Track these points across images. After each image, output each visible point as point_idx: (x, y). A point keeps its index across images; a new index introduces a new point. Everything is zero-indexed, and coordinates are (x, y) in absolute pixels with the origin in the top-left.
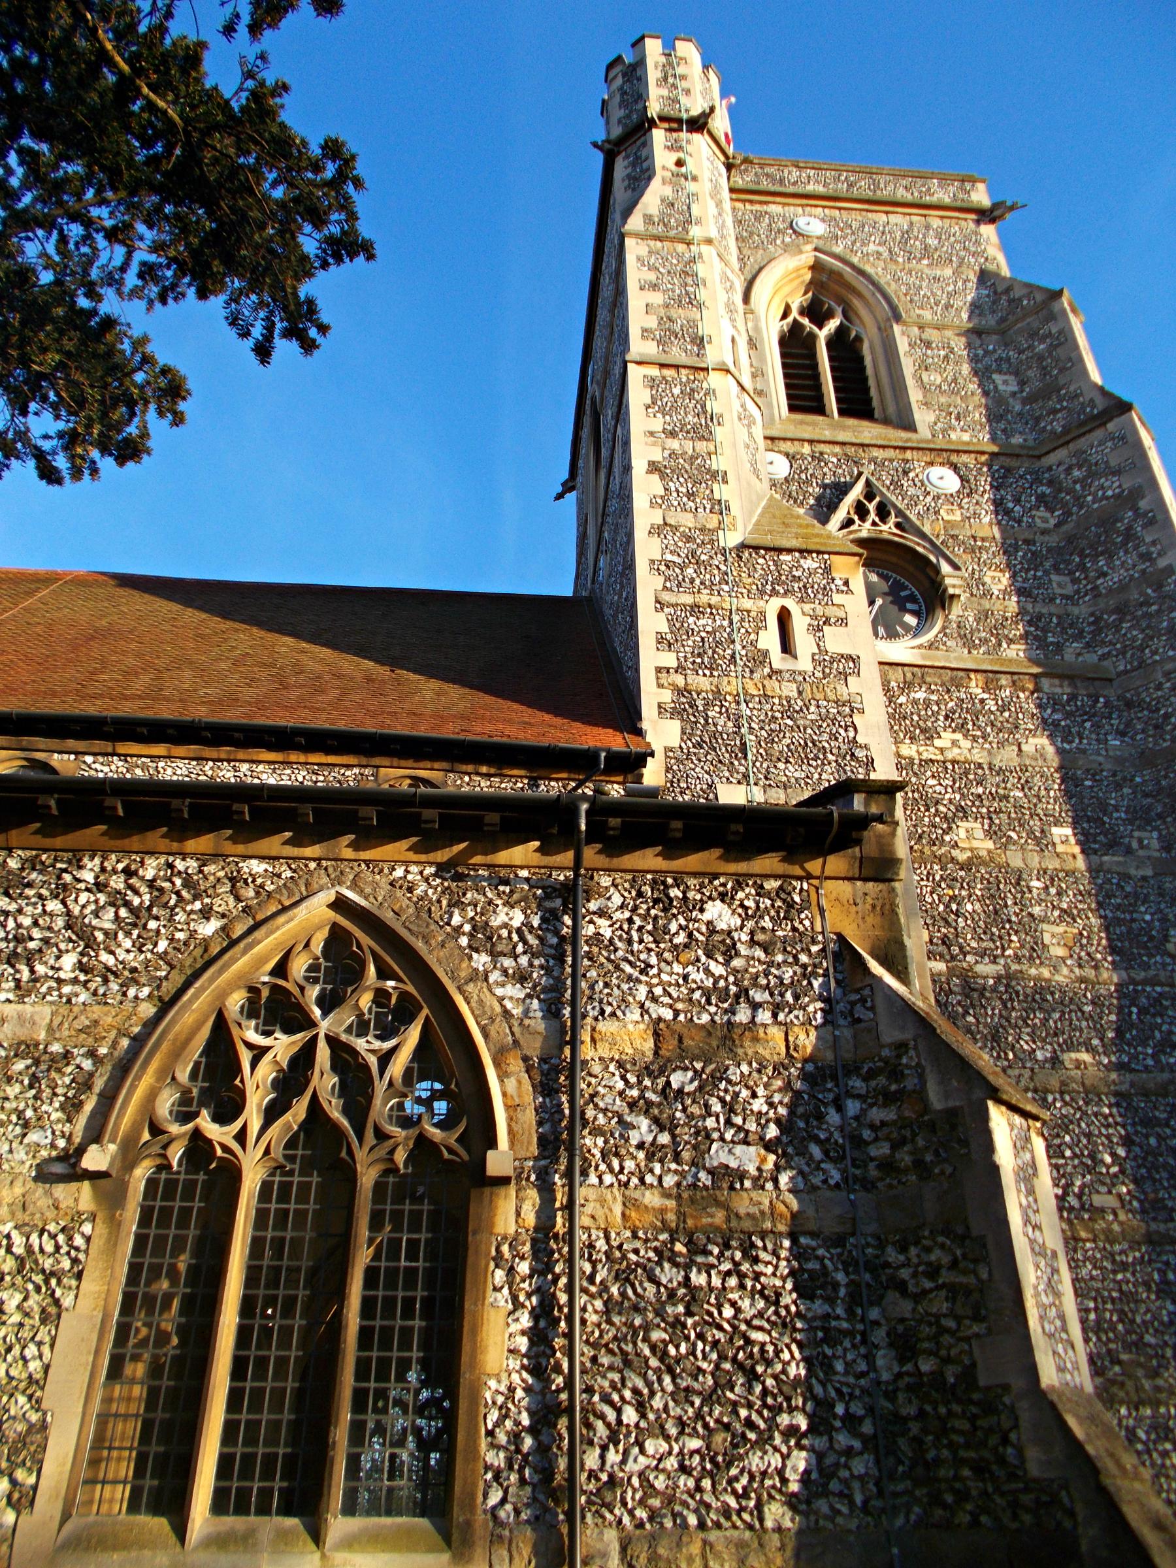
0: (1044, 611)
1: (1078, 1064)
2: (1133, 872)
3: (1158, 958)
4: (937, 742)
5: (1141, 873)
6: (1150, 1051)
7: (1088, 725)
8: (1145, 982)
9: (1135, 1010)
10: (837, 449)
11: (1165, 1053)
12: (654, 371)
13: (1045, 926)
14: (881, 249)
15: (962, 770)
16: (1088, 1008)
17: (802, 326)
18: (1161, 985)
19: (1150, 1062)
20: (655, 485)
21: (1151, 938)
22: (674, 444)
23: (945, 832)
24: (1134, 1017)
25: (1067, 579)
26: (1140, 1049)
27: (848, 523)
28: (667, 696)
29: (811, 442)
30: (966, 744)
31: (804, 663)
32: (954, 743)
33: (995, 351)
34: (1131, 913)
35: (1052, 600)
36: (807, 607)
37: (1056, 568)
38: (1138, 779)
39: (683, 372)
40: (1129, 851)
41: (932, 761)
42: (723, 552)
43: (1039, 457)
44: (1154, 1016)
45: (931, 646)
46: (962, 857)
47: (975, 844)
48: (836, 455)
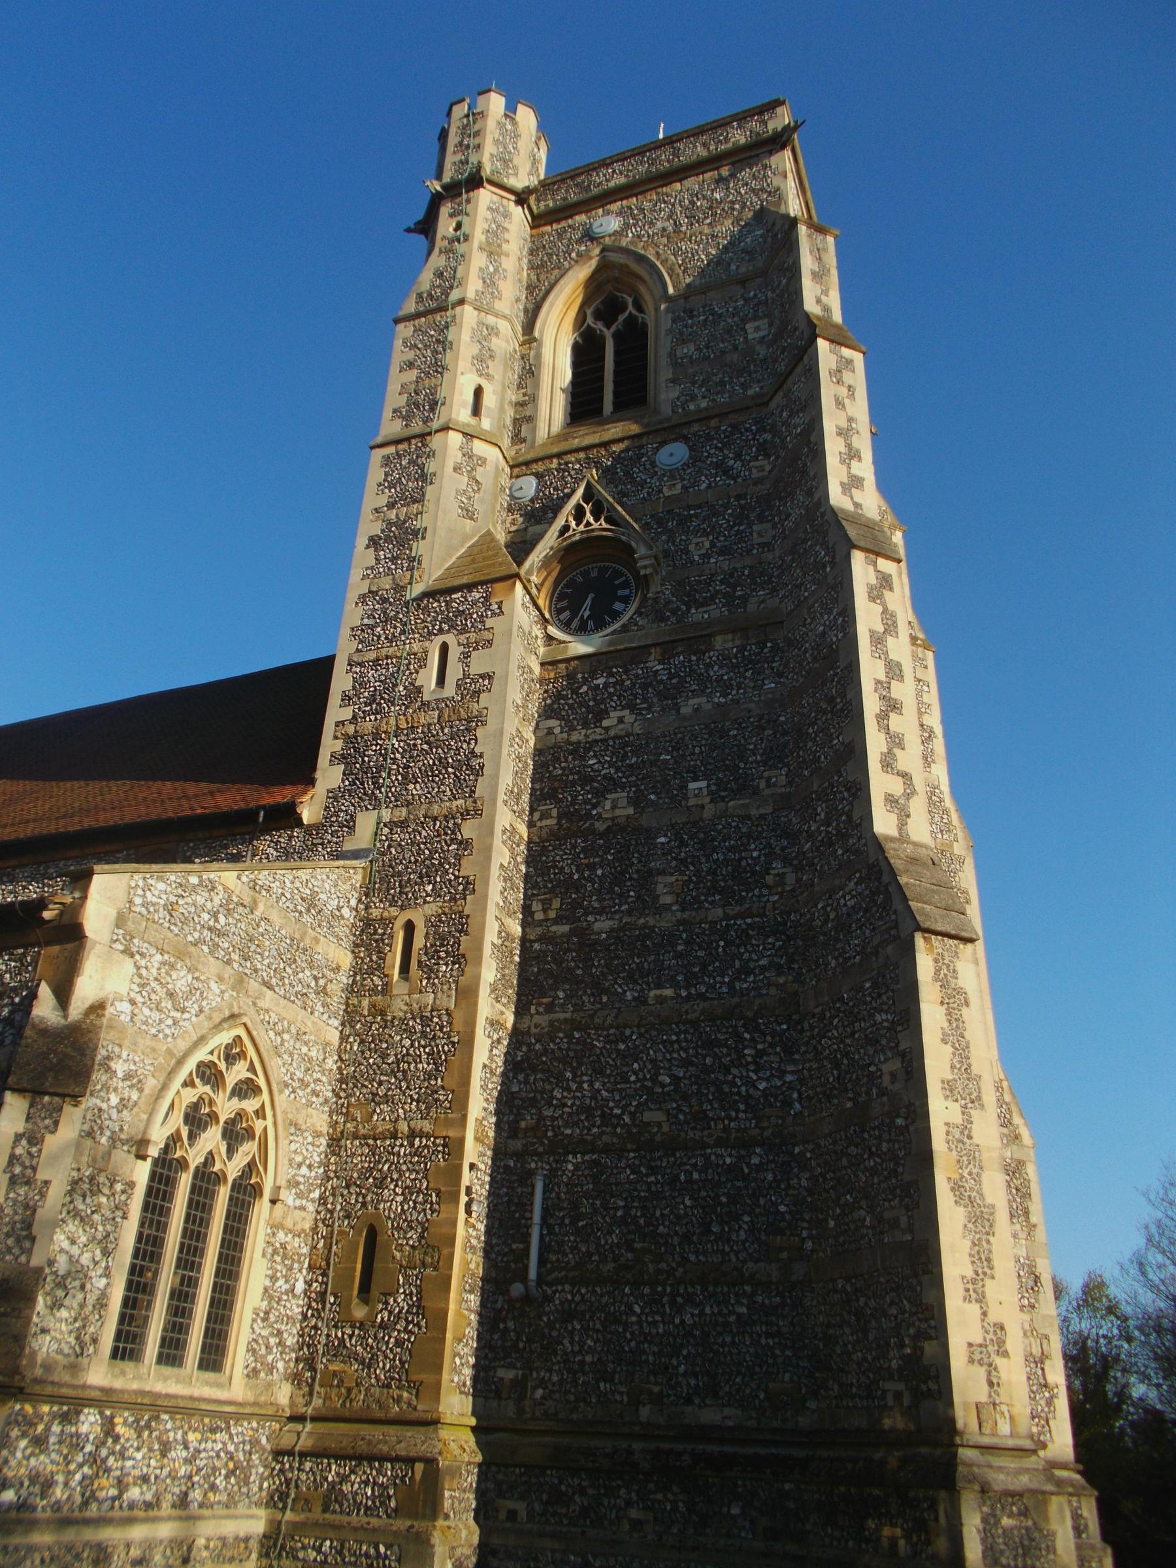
0: (738, 565)
1: (661, 1000)
2: (754, 812)
3: (756, 892)
4: (605, 723)
5: (762, 811)
6: (726, 980)
7: (749, 674)
8: (735, 917)
9: (722, 943)
10: (582, 455)
11: (740, 980)
12: (391, 450)
13: (660, 879)
14: (667, 224)
15: (621, 744)
16: (680, 948)
17: (594, 330)
18: (752, 917)
19: (725, 989)
20: (369, 557)
21: (754, 873)
22: (392, 515)
23: (594, 806)
24: (720, 950)
25: (769, 525)
26: (718, 979)
27: (566, 528)
28: (338, 745)
29: (559, 456)
30: (629, 717)
31: (450, 690)
32: (621, 720)
33: (755, 295)
34: (740, 852)
35: (749, 552)
36: (463, 639)
37: (761, 519)
38: (782, 719)
39: (413, 441)
40: (756, 792)
41: (596, 741)
42: (407, 604)
43: (767, 404)
44: (738, 946)
45: (625, 628)
46: (600, 826)
47: (618, 812)
48: (578, 461)
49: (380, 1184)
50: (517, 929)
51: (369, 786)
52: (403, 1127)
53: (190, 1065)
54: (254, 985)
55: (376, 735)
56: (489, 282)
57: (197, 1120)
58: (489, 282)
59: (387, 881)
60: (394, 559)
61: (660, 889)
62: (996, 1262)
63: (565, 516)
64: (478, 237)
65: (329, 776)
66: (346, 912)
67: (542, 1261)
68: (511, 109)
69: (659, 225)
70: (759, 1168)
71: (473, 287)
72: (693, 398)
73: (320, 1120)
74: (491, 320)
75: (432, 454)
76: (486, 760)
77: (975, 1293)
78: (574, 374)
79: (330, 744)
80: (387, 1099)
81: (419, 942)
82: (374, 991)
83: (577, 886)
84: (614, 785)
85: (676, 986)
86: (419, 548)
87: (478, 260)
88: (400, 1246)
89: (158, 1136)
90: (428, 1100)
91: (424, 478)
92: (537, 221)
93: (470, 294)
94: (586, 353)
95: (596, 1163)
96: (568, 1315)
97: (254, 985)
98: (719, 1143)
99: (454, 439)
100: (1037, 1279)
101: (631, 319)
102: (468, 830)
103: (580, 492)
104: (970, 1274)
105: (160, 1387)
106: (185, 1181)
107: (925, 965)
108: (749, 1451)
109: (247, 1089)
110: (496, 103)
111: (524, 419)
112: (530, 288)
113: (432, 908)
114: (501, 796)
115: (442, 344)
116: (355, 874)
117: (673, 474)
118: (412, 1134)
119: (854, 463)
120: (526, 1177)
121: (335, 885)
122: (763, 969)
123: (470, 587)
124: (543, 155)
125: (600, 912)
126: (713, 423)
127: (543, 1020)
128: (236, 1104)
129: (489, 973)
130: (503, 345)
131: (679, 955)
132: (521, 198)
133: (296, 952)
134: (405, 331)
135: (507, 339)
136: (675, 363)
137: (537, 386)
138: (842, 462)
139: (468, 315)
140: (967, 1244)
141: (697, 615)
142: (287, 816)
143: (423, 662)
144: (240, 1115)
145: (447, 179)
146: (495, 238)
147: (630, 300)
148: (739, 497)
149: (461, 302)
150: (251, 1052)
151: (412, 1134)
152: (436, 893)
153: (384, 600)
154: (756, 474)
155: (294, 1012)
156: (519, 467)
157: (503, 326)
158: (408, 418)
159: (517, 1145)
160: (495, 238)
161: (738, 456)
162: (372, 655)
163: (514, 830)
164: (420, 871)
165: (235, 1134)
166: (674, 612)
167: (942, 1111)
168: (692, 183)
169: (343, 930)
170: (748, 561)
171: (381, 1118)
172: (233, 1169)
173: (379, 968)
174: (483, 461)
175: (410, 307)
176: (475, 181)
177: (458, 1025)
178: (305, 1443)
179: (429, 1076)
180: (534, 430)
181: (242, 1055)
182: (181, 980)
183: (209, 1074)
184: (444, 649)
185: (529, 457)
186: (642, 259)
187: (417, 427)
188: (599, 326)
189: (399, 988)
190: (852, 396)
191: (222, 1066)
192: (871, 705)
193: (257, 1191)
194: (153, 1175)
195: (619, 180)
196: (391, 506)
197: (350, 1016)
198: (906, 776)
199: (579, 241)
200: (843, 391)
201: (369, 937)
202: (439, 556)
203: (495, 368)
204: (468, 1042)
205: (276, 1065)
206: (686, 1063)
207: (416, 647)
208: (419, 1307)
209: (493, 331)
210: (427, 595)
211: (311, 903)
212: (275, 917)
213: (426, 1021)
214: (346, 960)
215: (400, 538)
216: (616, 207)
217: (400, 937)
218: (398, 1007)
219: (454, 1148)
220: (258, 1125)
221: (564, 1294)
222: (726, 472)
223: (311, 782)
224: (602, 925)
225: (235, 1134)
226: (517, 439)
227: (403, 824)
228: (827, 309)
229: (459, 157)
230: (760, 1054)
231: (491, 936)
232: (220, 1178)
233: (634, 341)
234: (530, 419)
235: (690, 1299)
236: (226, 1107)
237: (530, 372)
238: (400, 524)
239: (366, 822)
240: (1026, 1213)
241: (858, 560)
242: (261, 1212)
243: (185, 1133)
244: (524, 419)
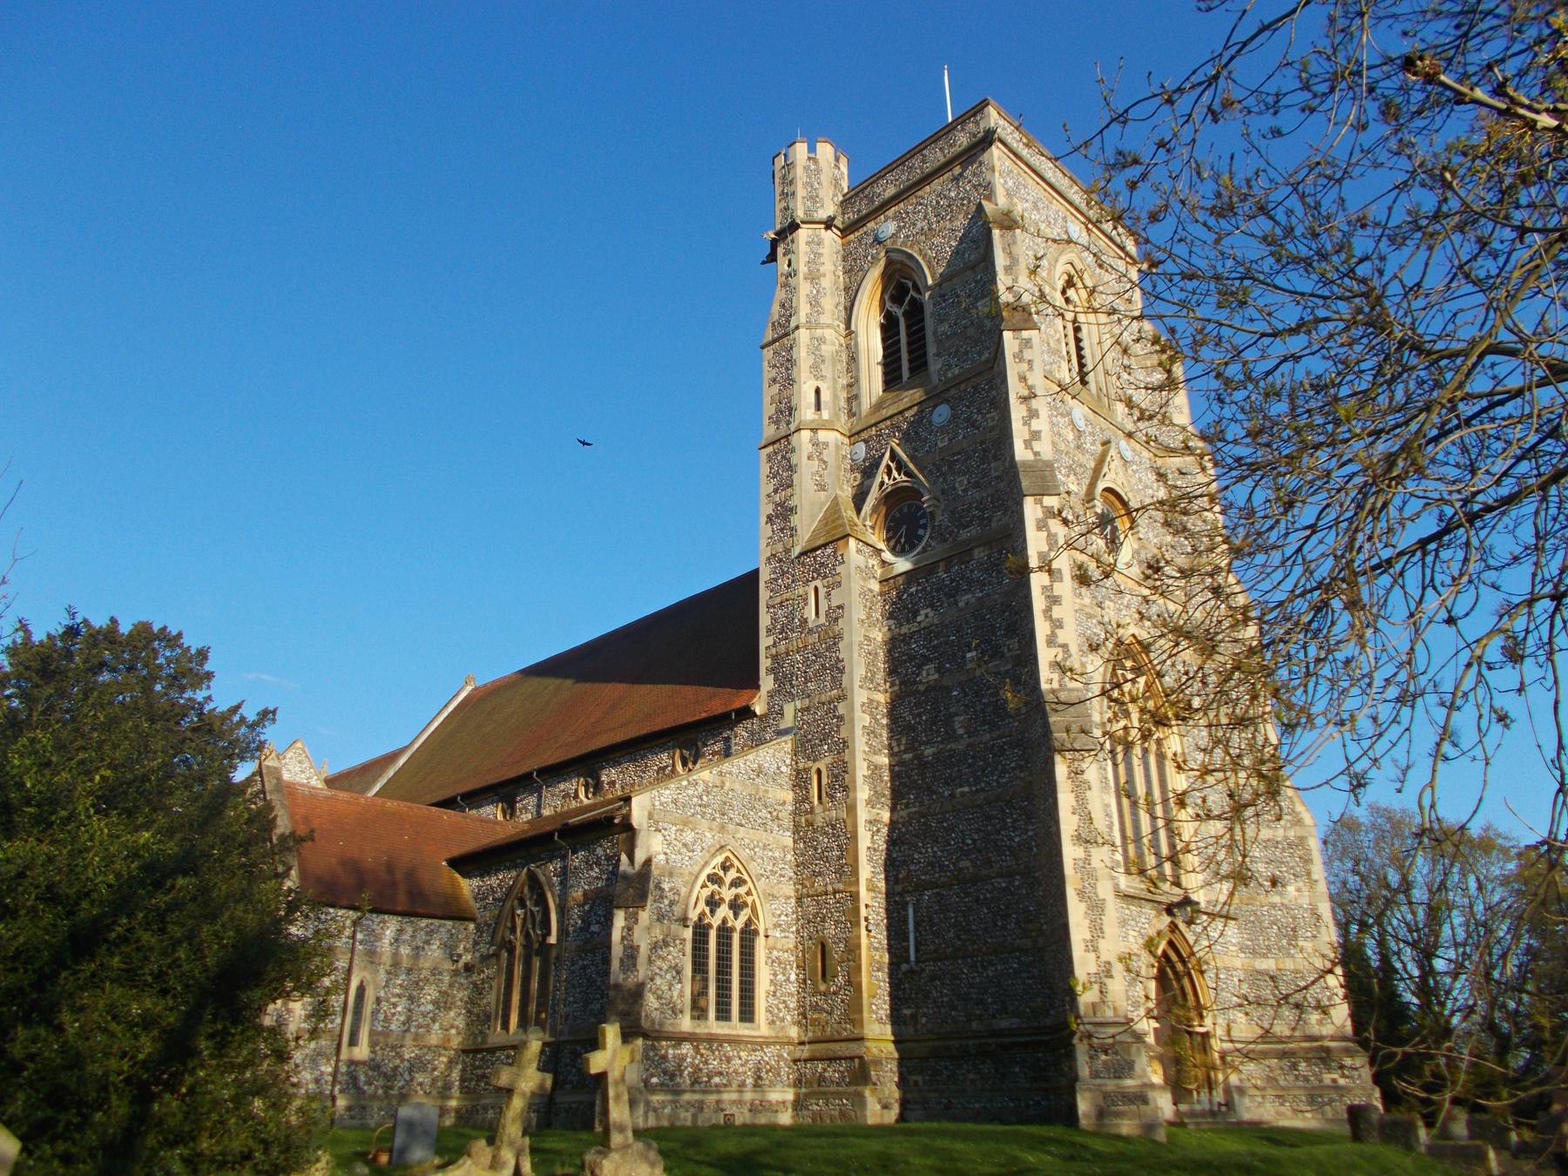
1: (963, 794)
12: (770, 449)
15: (928, 633)
27: (882, 483)
29: (875, 425)
31: (822, 619)
40: (1003, 655)
45: (924, 550)
46: (922, 688)
49: (823, 920)
50: (884, 760)
51: (788, 686)
52: (830, 888)
53: (703, 877)
54: (731, 827)
55: (787, 654)
56: (815, 303)
57: (713, 903)
58: (815, 303)
59: (805, 747)
60: (782, 530)
61: (957, 725)
62: (1106, 929)
63: (881, 475)
64: (803, 269)
65: (767, 683)
66: (784, 769)
67: (917, 950)
68: (812, 149)
69: (919, 225)
70: (1018, 888)
71: (804, 310)
72: (950, 367)
73: (789, 889)
74: (819, 332)
75: (793, 450)
76: (846, 663)
77: (1092, 946)
78: (885, 349)
79: (765, 663)
80: (820, 874)
81: (825, 781)
82: (806, 812)
83: (912, 728)
84: (926, 660)
85: (970, 785)
86: (795, 520)
87: (805, 288)
88: (837, 951)
89: (693, 916)
90: (839, 872)
91: (791, 468)
92: (845, 232)
93: (803, 320)
94: (889, 329)
95: (938, 894)
96: (933, 978)
97: (731, 827)
98: (1000, 875)
99: (805, 435)
100: (1319, 918)
101: (913, 300)
102: (841, 709)
103: (888, 455)
104: (1088, 937)
105: (719, 1031)
106: (713, 935)
107: (1061, 769)
108: (1022, 1039)
109: (738, 883)
110: (801, 149)
112: (846, 289)
113: (828, 760)
114: (857, 683)
115: (790, 363)
116: (786, 744)
117: (942, 429)
118: (835, 892)
119: (1034, 422)
120: (905, 906)
121: (776, 756)
122: (1014, 769)
123: (825, 545)
124: (844, 168)
125: (927, 743)
126: (963, 386)
127: (904, 813)
128: (734, 891)
129: (863, 793)
130: (835, 341)
131: (970, 766)
132: (829, 224)
133: (756, 800)
134: (768, 353)
135: (833, 338)
136: (939, 341)
137: (858, 370)
138: (1025, 423)
139: (803, 335)
140: (1087, 922)
141: (964, 534)
142: (746, 713)
143: (806, 600)
144: (737, 896)
145: (778, 227)
146: (818, 253)
147: (910, 285)
148: (982, 443)
149: (797, 328)
150: (736, 863)
151: (835, 892)
152: (830, 750)
153: (780, 560)
154: (991, 424)
155: (762, 835)
156: (854, 436)
157: (829, 334)
158: (777, 422)
159: (899, 888)
160: (818, 253)
161: (979, 411)
162: (778, 600)
163: (871, 701)
164: (821, 737)
165: (736, 906)
166: (951, 533)
167: (1071, 852)
168: (936, 185)
169: (785, 780)
170: (990, 491)
171: (819, 883)
172: (739, 924)
173: (806, 799)
174: (826, 444)
175: (769, 336)
176: (794, 227)
177: (850, 828)
178: (806, 1055)
179: (839, 858)
180: (859, 405)
181: (732, 865)
182: (689, 836)
183: (714, 879)
184: (816, 589)
185: (858, 428)
186: (910, 256)
187: (783, 430)
189: (818, 810)
190: (1031, 368)
191: (721, 873)
192: (1038, 603)
193: (756, 932)
194: (695, 934)
195: (891, 191)
196: (776, 491)
197: (797, 828)
198: (1065, 646)
199: (872, 245)
200: (1025, 366)
201: (800, 781)
202: (806, 526)
203: (826, 370)
204: (854, 837)
205: (754, 868)
206: (978, 831)
207: (801, 591)
208: (849, 982)
209: (822, 340)
210: (803, 553)
211: (759, 771)
212: (737, 787)
213: (834, 827)
214: (789, 796)
215: (783, 513)
216: (890, 213)
217: (815, 778)
218: (819, 821)
219: (855, 897)
220: (749, 900)
221: (930, 967)
222: (973, 425)
223: (758, 687)
224: (929, 751)
225: (736, 906)
226: (851, 414)
227: (808, 709)
229: (783, 204)
230: (1015, 821)
231: (861, 770)
232: (732, 929)
234: (856, 397)
235: (991, 963)
236: (728, 894)
237: (853, 359)
238: (781, 504)
239: (789, 710)
240: (1309, 874)
241: (1029, 503)
242: (760, 945)
243: (707, 910)
244: (853, 398)
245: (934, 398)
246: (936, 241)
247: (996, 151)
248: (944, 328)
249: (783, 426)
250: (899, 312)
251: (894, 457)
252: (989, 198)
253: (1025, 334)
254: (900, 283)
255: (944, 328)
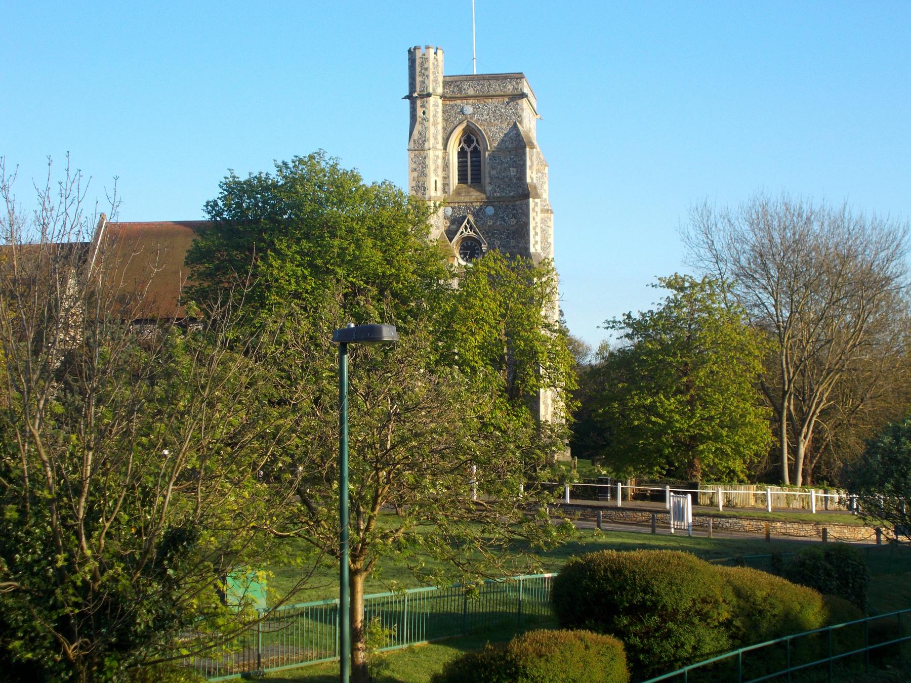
63: (462, 229)
64: (431, 120)
94: (462, 154)
111: (446, 185)
117: (490, 217)
135: (440, 153)
168: (495, 101)
186: (480, 130)
188: (466, 147)
195: (471, 92)
216: (471, 101)
222: (504, 220)
228: (532, 179)
233: (476, 153)
234: (448, 185)
237: (446, 166)
245: (489, 202)
246: (494, 129)
247: (525, 100)
248: (494, 172)
249: (420, 194)
250: (469, 150)
251: (468, 222)
252: (521, 122)
253: (536, 200)
254: (470, 137)
255: (494, 172)
